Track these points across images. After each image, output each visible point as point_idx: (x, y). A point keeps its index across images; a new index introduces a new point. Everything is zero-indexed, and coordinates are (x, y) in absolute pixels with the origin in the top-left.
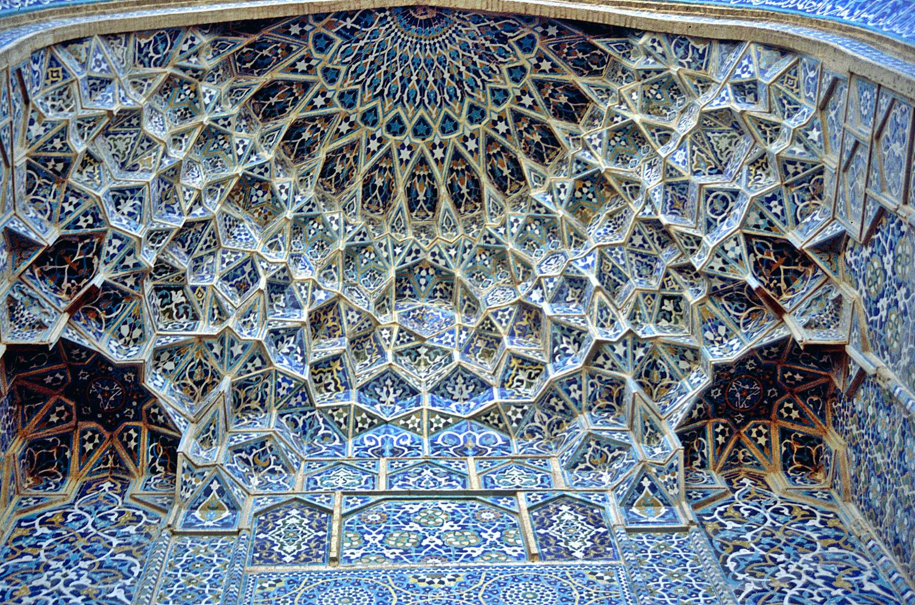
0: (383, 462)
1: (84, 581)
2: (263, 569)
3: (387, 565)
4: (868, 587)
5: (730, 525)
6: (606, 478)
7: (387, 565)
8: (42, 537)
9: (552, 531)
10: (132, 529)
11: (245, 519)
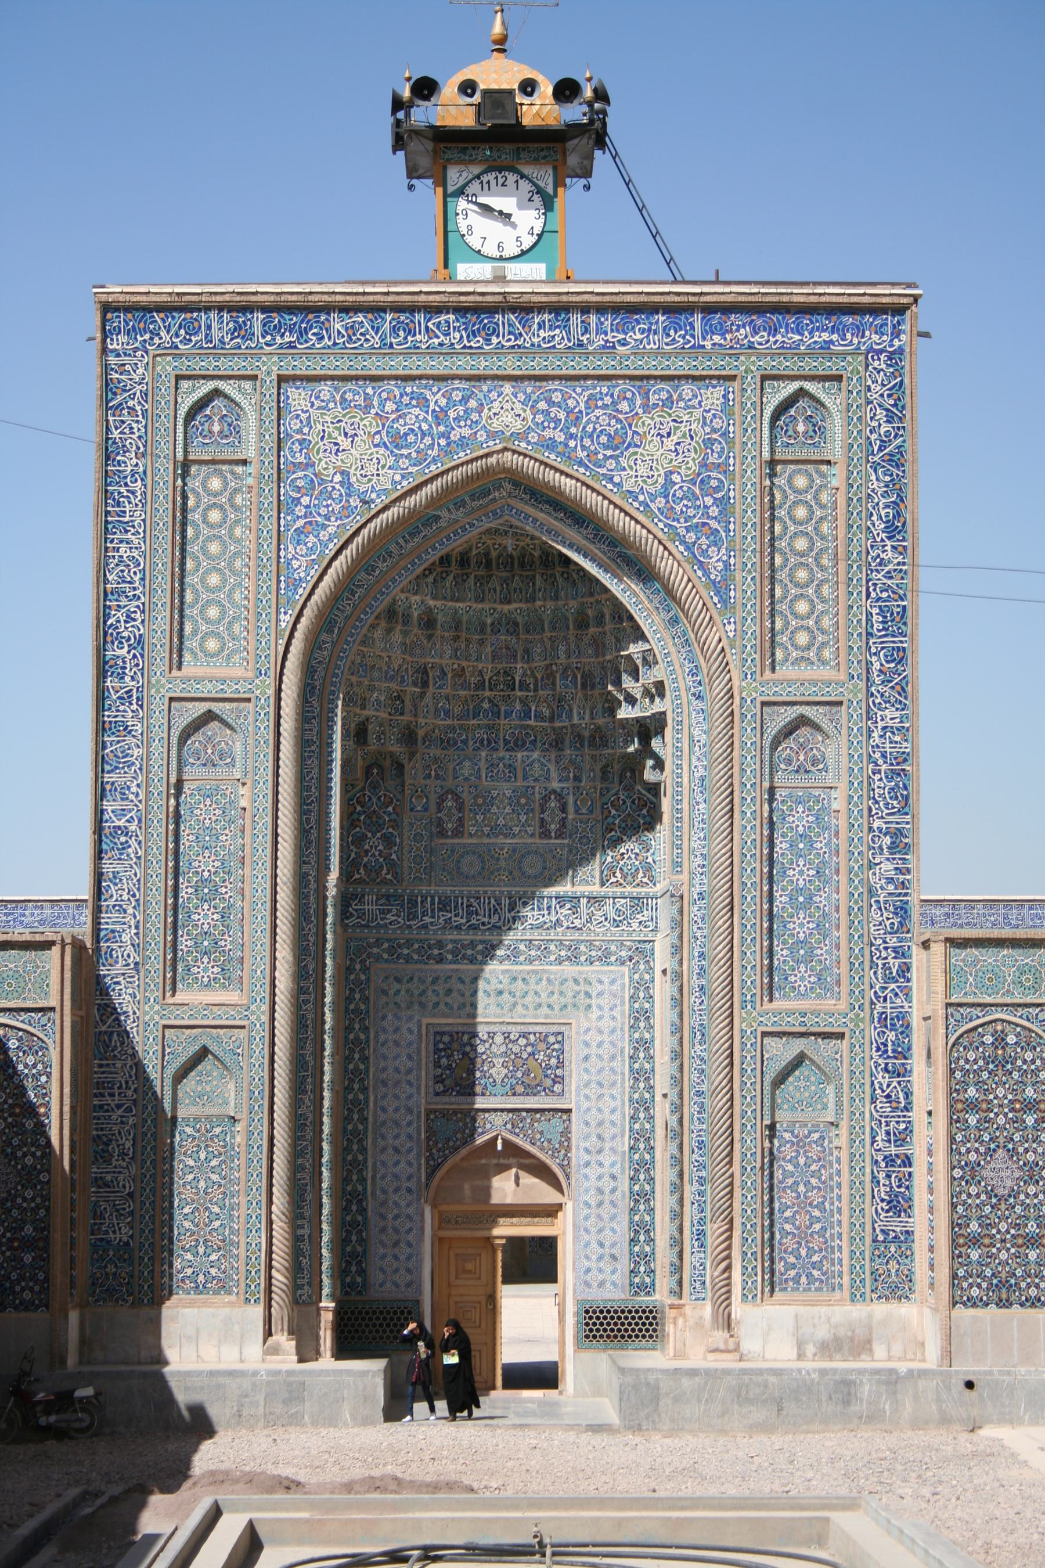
0: (483, 754)
1: (381, 847)
2: (442, 841)
3: (486, 841)
4: (650, 860)
5: (613, 812)
6: (571, 775)
7: (486, 841)
8: (359, 814)
9: (545, 816)
10: (390, 809)
11: (433, 807)
